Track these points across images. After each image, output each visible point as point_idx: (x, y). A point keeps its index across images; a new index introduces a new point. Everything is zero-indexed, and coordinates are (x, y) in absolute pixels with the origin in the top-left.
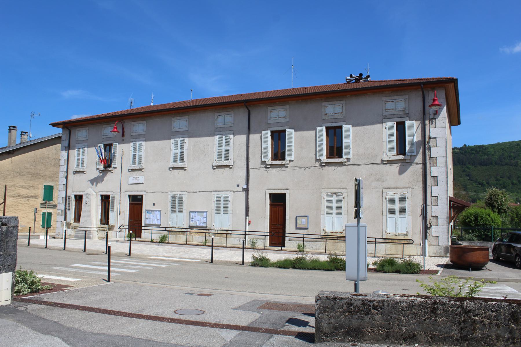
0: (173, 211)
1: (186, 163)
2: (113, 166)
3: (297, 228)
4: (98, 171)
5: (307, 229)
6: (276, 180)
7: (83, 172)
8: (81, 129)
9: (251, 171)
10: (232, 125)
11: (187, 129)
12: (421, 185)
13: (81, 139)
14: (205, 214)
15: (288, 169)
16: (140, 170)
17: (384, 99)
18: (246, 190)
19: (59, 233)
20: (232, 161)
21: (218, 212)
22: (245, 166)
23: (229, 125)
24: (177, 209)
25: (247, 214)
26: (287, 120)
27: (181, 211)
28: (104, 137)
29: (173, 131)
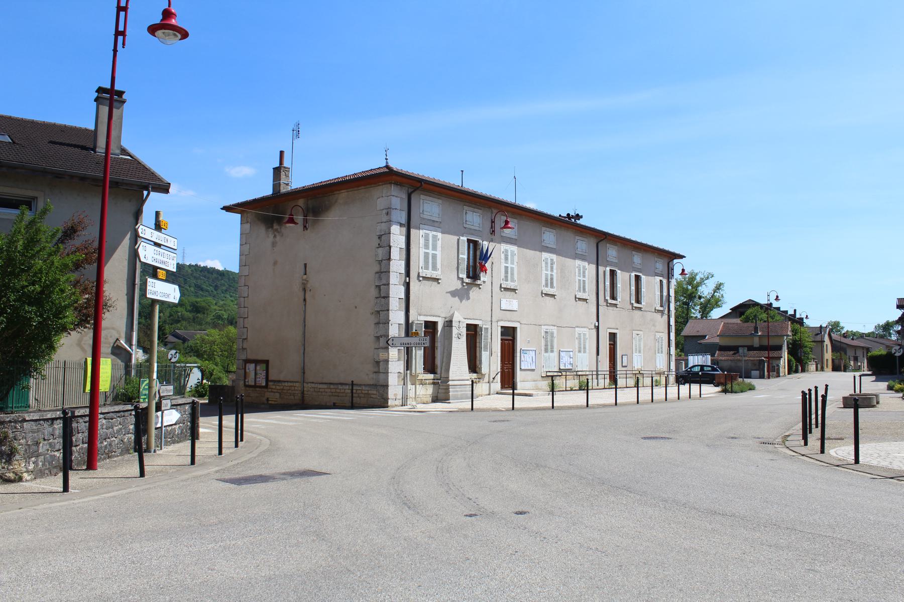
1: (555, 290)
2: (482, 279)
4: (459, 282)
6: (611, 320)
7: (437, 280)
8: (431, 198)
13: (429, 218)
16: (514, 290)
18: (598, 328)
19: (395, 395)
21: (580, 351)
22: (595, 302)
24: (549, 347)
25: (598, 354)
27: (552, 351)
28: (467, 226)
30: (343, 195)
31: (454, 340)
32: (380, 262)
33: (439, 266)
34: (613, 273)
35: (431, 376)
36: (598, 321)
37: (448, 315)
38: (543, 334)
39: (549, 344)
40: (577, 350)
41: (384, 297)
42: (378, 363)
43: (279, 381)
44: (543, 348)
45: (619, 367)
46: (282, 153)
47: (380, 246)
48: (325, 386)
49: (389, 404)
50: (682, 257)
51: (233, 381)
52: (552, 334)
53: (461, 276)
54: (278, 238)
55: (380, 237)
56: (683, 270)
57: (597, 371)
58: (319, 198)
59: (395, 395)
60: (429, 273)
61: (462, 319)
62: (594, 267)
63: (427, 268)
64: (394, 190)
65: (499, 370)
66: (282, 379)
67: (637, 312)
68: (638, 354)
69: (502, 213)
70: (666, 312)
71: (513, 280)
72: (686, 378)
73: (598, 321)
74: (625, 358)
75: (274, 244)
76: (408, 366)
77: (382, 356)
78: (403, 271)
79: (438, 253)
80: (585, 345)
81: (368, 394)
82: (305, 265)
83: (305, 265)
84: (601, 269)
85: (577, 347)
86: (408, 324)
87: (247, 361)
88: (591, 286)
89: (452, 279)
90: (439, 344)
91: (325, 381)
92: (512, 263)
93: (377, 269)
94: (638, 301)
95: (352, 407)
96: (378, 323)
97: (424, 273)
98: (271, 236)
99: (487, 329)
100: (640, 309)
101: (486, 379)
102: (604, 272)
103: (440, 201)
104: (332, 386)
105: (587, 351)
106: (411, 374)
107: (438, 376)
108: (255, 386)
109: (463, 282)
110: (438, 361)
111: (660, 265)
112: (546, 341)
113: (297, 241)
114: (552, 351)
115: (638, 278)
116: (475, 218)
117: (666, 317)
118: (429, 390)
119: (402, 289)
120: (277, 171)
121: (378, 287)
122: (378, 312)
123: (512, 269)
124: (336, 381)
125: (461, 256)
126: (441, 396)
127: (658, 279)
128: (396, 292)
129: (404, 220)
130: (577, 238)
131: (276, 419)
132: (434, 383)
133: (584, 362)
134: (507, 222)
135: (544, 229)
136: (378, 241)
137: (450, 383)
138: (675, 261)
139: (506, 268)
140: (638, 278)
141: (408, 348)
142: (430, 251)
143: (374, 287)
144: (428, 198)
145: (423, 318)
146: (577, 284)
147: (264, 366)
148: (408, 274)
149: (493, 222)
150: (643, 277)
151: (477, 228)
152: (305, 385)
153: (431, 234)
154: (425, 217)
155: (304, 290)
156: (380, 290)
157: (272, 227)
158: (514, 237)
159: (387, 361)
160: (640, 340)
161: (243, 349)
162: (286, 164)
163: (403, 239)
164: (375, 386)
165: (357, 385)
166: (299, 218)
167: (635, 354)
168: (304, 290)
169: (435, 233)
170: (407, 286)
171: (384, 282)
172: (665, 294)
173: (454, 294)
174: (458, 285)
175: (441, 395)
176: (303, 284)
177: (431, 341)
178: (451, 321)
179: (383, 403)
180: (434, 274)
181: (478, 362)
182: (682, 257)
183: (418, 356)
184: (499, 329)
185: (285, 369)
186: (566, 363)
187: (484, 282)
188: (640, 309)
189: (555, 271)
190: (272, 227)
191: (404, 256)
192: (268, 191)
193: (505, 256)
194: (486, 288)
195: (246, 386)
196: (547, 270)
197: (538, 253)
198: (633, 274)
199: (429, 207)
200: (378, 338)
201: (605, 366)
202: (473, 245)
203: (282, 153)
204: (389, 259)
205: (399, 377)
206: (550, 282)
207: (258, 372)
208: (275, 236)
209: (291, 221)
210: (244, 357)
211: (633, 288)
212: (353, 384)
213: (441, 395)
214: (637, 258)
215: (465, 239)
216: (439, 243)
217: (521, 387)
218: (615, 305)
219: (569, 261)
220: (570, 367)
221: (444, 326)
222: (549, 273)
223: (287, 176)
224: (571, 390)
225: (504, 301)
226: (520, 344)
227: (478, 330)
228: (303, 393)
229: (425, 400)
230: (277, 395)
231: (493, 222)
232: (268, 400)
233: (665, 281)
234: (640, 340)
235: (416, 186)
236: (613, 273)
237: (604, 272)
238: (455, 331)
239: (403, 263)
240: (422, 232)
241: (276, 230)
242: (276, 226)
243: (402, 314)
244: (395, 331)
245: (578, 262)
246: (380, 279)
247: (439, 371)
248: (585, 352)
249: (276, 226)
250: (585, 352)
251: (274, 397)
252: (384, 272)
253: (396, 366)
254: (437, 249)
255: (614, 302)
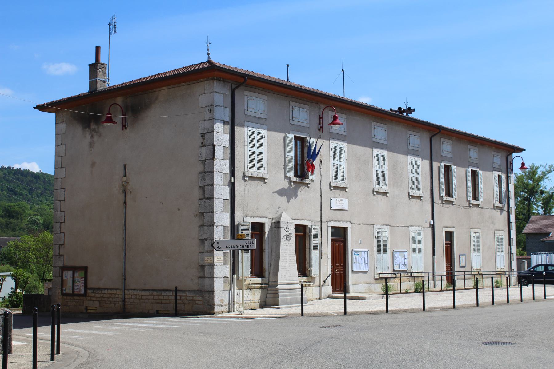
0: (379, 251)
1: (387, 187)
2: (311, 177)
3: (460, 267)
5: (464, 267)
6: (447, 218)
7: (263, 179)
8: (255, 94)
9: (434, 204)
10: (420, 150)
11: (386, 142)
12: (507, 229)
13: (254, 115)
14: (406, 254)
15: (454, 206)
16: (344, 189)
17: (493, 153)
18: (433, 227)
19: (222, 301)
20: (421, 191)
21: (414, 252)
23: (417, 149)
24: (382, 248)
25: (434, 254)
26: (452, 156)
27: (385, 252)
28: (293, 123)
29: (374, 140)
30: (164, 92)
31: (282, 241)
32: (203, 162)
33: (265, 164)
34: (448, 169)
35: (259, 280)
36: (433, 219)
37: (276, 216)
38: (375, 234)
39: (382, 244)
40: (411, 250)
41: (208, 199)
42: (203, 267)
43: (99, 289)
44: (376, 249)
45: (457, 268)
46: (98, 49)
47: (203, 145)
48: (147, 293)
49: (215, 310)
50: (521, 150)
51: (50, 290)
52: (385, 233)
53: (288, 175)
54: (96, 138)
55: (203, 136)
56: (523, 164)
57: (433, 272)
58: (139, 96)
59: (222, 301)
60: (255, 172)
61: (290, 220)
62: (427, 162)
63: (252, 167)
64: (217, 86)
65: (330, 272)
66: (101, 286)
67: (474, 209)
68: (476, 254)
69: (330, 109)
70: (506, 208)
71: (342, 178)
72: (528, 278)
73: (433, 219)
74: (462, 258)
75: (91, 145)
76: (235, 270)
77: (207, 259)
78: (227, 170)
79: (264, 151)
80: (419, 245)
81: (193, 300)
82: (125, 166)
83: (125, 166)
84: (435, 165)
85: (411, 247)
86: (234, 226)
87: (64, 268)
88: (425, 183)
89: (279, 179)
90: (266, 247)
91: (147, 287)
92: (342, 160)
93: (200, 168)
94: (475, 198)
95: (177, 314)
96: (202, 226)
97: (250, 172)
98: (88, 137)
99: (317, 229)
100: (477, 206)
101: (317, 282)
102: (439, 168)
103: (265, 97)
104: (155, 293)
105: (423, 251)
106: (237, 279)
107: (266, 280)
108: (73, 295)
109: (290, 181)
110: (266, 265)
111: (498, 159)
112: (379, 242)
113: (115, 141)
114: (385, 252)
115: (474, 173)
116: (302, 114)
117: (505, 214)
118: (257, 295)
119: (227, 190)
120: (94, 68)
121: (202, 188)
122: (202, 214)
123: (342, 166)
124: (159, 287)
125: (288, 154)
126: (269, 301)
127: (496, 174)
128: (221, 192)
129: (227, 118)
130: (409, 132)
131: (96, 329)
132: (262, 288)
133: (420, 263)
134: (335, 118)
135: (374, 124)
136: (201, 140)
137: (279, 287)
138: (514, 155)
139: (336, 165)
140: (474, 174)
141: (234, 251)
142: (256, 150)
143: (197, 187)
144: (253, 94)
145: (249, 220)
146: (410, 181)
147: (82, 273)
148: (233, 173)
149: (321, 118)
150: (480, 173)
151: (304, 125)
152: (126, 292)
153: (256, 131)
154: (250, 114)
155: (125, 192)
156: (204, 191)
157: (89, 126)
158: (343, 133)
159: (212, 265)
160: (478, 239)
161: (60, 255)
162: (103, 59)
163: (226, 138)
164: (200, 292)
165: (181, 291)
166: (118, 117)
167: (473, 254)
168: (125, 192)
169: (260, 131)
170: (232, 186)
171: (208, 182)
172: (504, 189)
173: (281, 192)
174: (285, 184)
175: (269, 300)
176: (124, 186)
177: (258, 243)
178: (278, 223)
179: (207, 309)
180: (261, 174)
181: (307, 265)
182: (521, 150)
183: (245, 259)
184: (330, 229)
185: (105, 277)
186: (400, 264)
187: (313, 181)
188: (477, 206)
189: (386, 168)
190: (89, 126)
191: (228, 155)
192: (84, 89)
193: (332, 153)
194: (315, 186)
195: (63, 294)
196: (378, 167)
197: (368, 149)
198: (469, 169)
199: (254, 103)
200: (202, 241)
201: (441, 266)
202: (301, 142)
203: (98, 49)
204: (213, 158)
205: (225, 282)
206: (381, 180)
207: (76, 279)
208: (92, 136)
209: (110, 120)
210: (61, 264)
211: (470, 184)
212: (176, 290)
213: (269, 300)
214: (474, 153)
215: (292, 136)
216: (265, 141)
217: (353, 290)
218: (451, 203)
219: (401, 158)
220: (404, 268)
221: (271, 228)
222: (381, 170)
223: (104, 73)
224: (407, 292)
225: (333, 201)
226: (351, 245)
227: (307, 231)
228: (124, 300)
229: (253, 305)
230: (97, 304)
231: (321, 118)
232: (86, 308)
233: (504, 176)
234: (478, 239)
235: (240, 82)
236: (448, 169)
237: (439, 168)
238: (283, 232)
239: (227, 163)
240: (247, 130)
241: (94, 130)
242: (93, 126)
243: (228, 216)
244: (219, 233)
245: (411, 158)
246: (204, 179)
247: (267, 274)
248: (420, 252)
249: (93, 126)
250: (420, 252)
251: (93, 306)
252: (207, 172)
253: (221, 270)
254: (264, 147)
255: (449, 199)
